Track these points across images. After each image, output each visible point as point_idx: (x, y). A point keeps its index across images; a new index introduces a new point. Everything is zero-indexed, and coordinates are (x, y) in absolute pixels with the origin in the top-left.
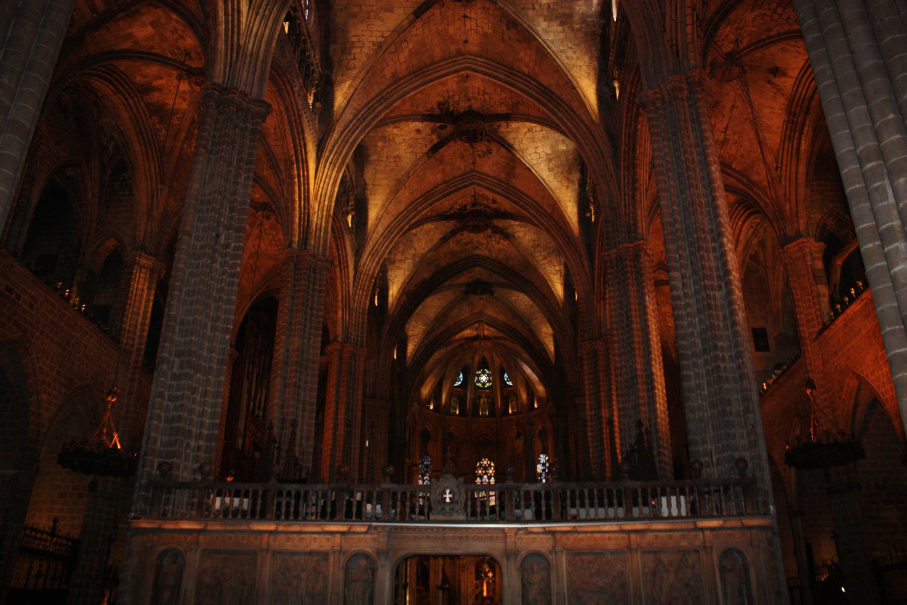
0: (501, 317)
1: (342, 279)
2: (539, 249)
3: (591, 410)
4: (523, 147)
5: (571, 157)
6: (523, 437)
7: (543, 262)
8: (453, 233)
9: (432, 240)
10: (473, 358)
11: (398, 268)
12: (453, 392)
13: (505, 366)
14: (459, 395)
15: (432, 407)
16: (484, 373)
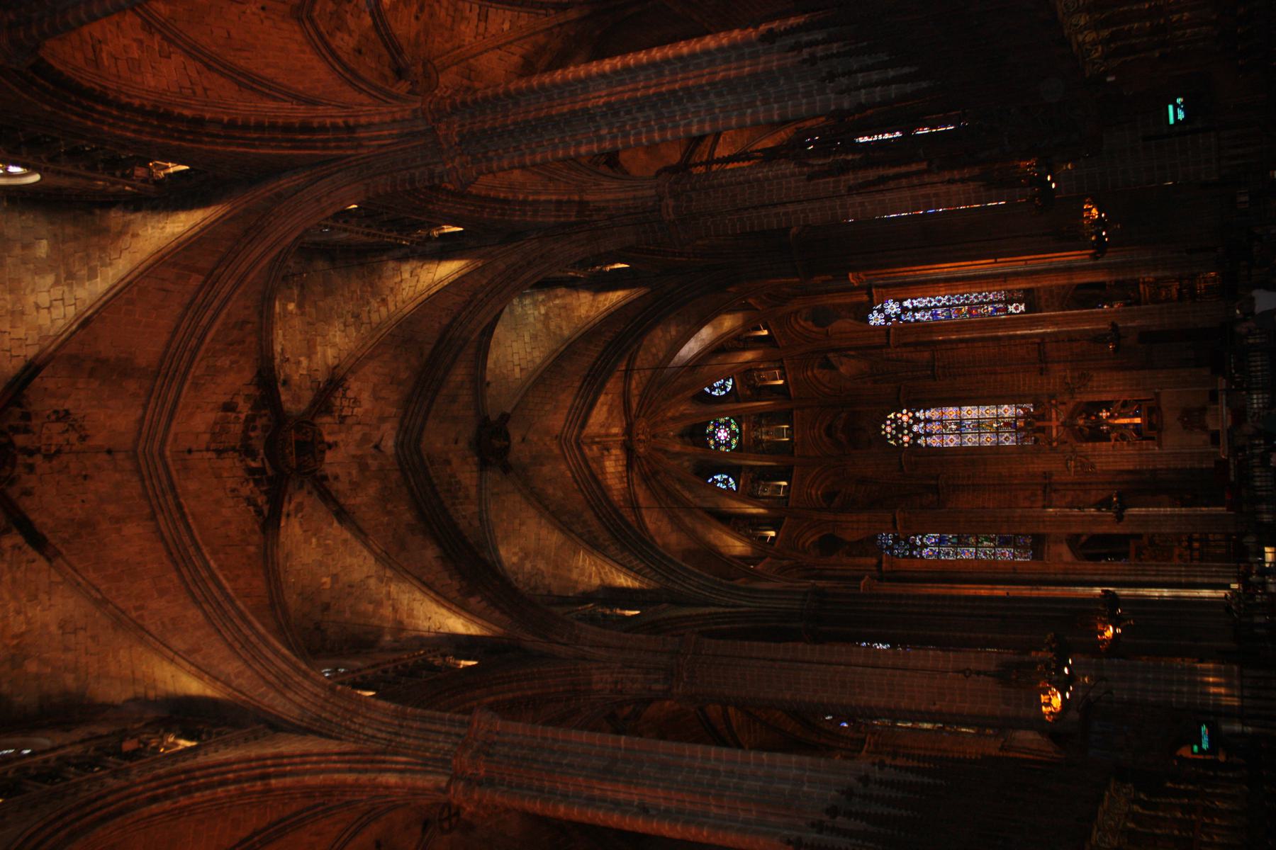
0: (567, 399)
1: (306, 772)
2: (364, 316)
3: (601, 139)
4: (33, 336)
5: (69, 230)
6: (830, 355)
7: (392, 308)
8: (327, 496)
9: (345, 541)
10: (678, 455)
11: (410, 614)
12: (749, 496)
13: (689, 394)
14: (753, 480)
15: (772, 534)
16: (713, 435)
